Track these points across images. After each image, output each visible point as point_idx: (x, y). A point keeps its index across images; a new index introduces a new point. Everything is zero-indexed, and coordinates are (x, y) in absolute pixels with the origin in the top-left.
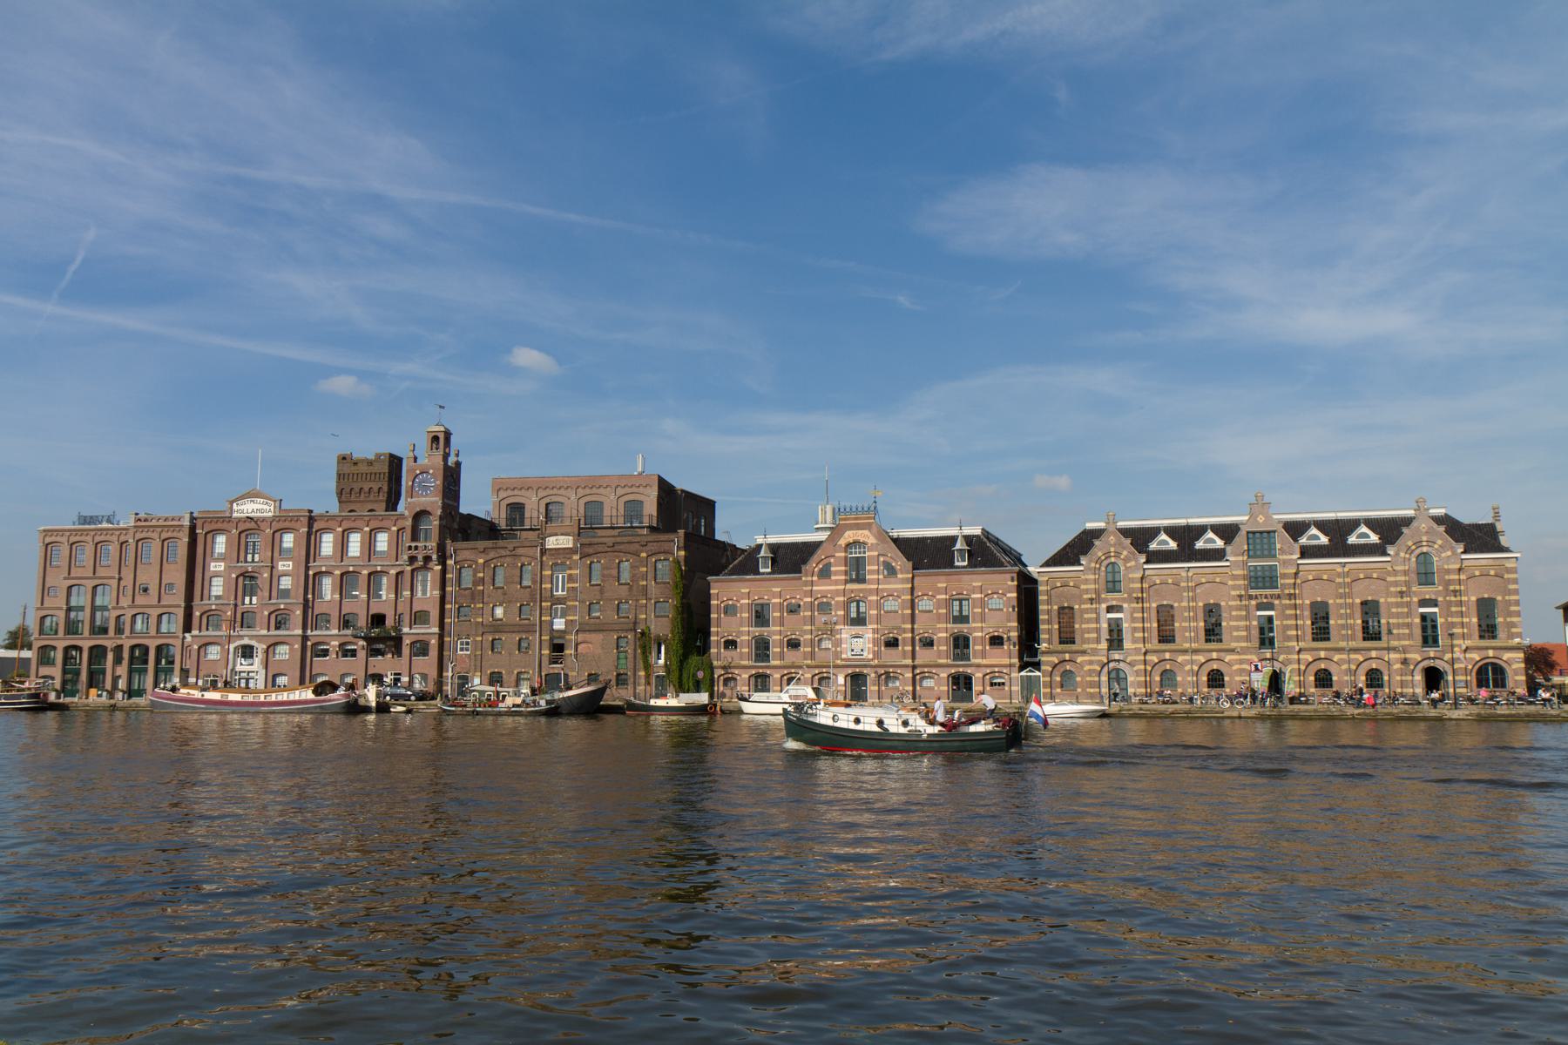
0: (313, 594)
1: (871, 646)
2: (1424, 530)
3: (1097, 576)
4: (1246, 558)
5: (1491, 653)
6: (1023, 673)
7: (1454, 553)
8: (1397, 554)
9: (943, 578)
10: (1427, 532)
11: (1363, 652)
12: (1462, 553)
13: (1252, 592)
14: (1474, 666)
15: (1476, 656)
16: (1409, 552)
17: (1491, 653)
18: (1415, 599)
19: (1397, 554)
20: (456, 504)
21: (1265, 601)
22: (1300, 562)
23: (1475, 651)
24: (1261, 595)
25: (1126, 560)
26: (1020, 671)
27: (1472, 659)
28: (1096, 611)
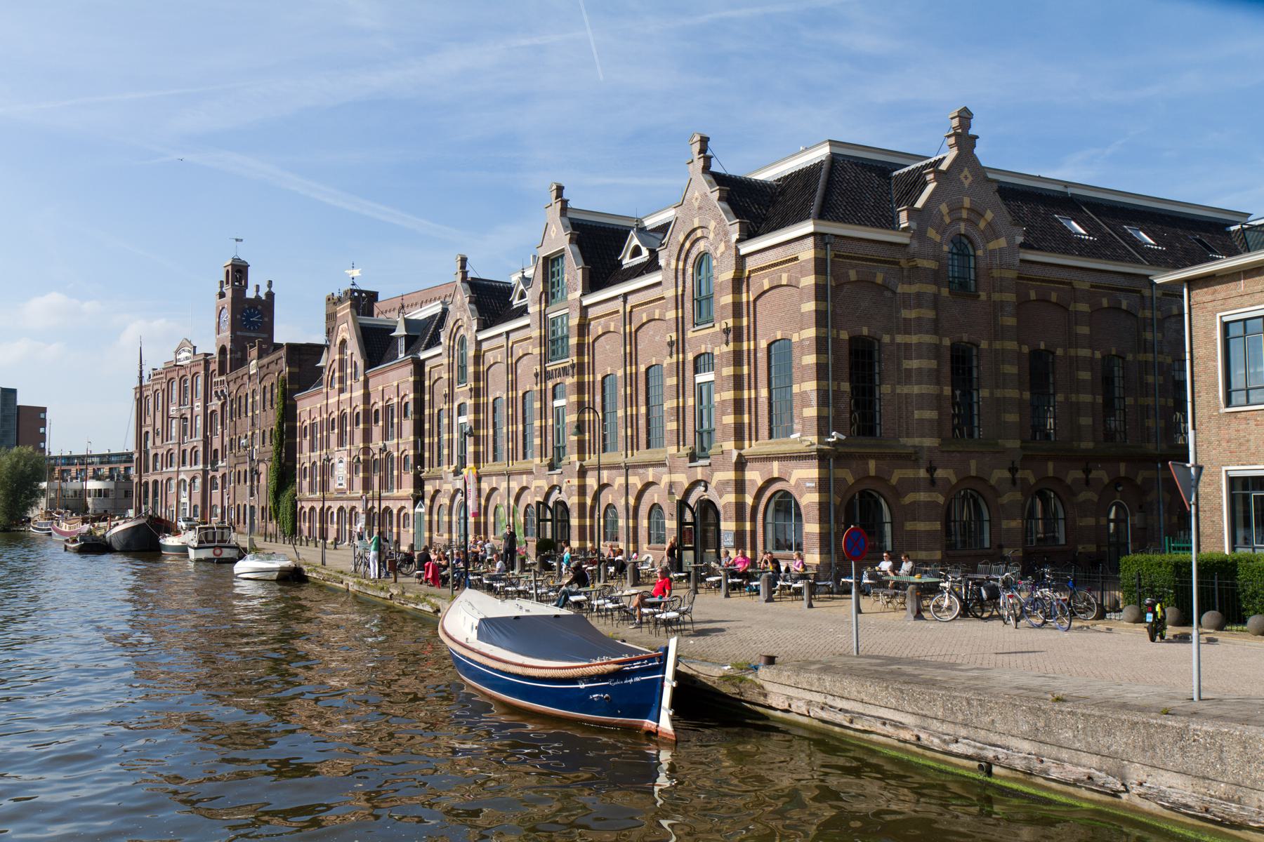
0: (211, 431)
1: (345, 472)
2: (696, 204)
3: (451, 359)
4: (543, 305)
5: (775, 469)
6: (417, 510)
7: (727, 242)
8: (668, 264)
9: (380, 377)
10: (700, 208)
11: (641, 471)
12: (739, 241)
13: (551, 366)
14: (758, 497)
15: (754, 476)
16: (683, 256)
17: (775, 469)
18: (690, 357)
19: (668, 264)
20: (239, 333)
21: (559, 380)
22: (586, 302)
23: (757, 464)
24: (556, 370)
25: (467, 329)
26: (414, 507)
27: (753, 481)
28: (450, 418)
